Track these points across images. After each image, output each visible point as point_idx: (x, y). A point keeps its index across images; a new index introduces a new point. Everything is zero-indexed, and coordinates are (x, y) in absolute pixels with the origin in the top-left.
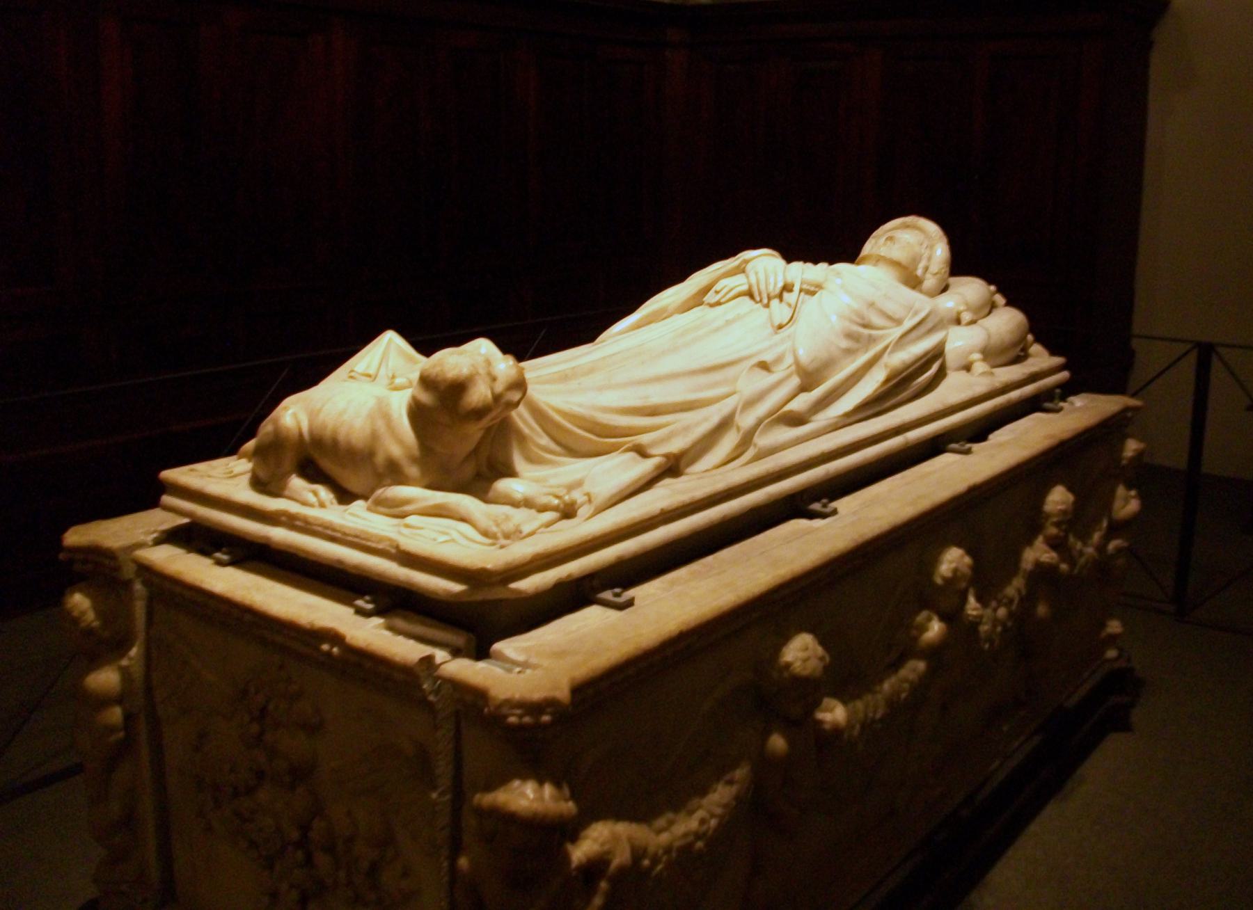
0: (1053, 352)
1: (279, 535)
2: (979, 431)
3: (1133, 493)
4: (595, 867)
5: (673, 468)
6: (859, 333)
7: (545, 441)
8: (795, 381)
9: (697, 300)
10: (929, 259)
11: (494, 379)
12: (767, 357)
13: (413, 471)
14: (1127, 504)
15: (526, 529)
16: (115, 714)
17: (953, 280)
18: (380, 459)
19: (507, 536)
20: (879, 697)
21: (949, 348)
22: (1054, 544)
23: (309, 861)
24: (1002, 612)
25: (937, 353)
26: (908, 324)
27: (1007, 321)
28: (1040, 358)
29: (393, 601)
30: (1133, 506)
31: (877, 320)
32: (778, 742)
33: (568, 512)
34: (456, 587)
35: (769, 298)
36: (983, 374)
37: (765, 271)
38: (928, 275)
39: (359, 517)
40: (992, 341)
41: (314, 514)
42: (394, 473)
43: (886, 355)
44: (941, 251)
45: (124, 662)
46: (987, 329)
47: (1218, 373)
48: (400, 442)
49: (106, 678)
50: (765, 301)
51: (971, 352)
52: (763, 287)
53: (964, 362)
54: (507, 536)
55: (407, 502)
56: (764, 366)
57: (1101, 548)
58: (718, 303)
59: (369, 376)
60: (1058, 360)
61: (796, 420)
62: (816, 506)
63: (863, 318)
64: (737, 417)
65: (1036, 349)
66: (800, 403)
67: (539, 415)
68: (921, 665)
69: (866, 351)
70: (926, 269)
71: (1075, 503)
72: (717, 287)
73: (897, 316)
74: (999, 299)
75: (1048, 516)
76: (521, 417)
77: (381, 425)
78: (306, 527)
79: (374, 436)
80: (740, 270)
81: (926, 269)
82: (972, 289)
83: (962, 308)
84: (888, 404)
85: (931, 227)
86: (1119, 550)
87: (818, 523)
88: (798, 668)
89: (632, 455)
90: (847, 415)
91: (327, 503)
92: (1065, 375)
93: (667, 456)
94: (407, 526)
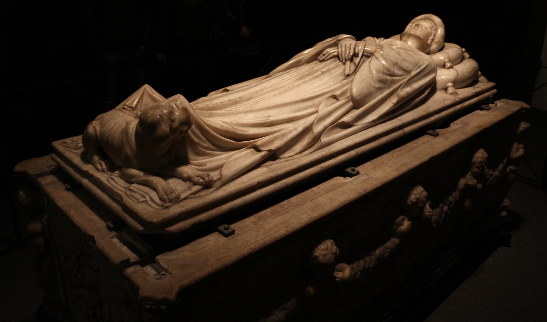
0: (489, 80)
1: (85, 181)
2: (445, 123)
3: (521, 146)
5: (273, 156)
6: (387, 79)
7: (207, 144)
8: (350, 104)
10: (435, 35)
11: (173, 121)
12: (337, 93)
14: (518, 151)
15: (183, 196)
16: (41, 240)
17: (446, 44)
19: (171, 201)
20: (373, 257)
21: (438, 79)
22: (475, 176)
24: (445, 208)
26: (413, 73)
27: (468, 66)
28: (483, 84)
30: (521, 152)
31: (397, 71)
32: (311, 290)
33: (207, 185)
34: (141, 228)
35: (346, 61)
36: (451, 94)
37: (346, 45)
38: (434, 43)
40: (459, 77)
43: (399, 90)
44: (440, 32)
45: (43, 220)
46: (457, 71)
48: (131, 148)
50: (344, 61)
51: (448, 82)
52: (343, 54)
53: (444, 86)
54: (171, 201)
55: (133, 176)
56: (335, 97)
58: (324, 60)
59: (132, 108)
60: (491, 84)
62: (349, 170)
63: (390, 72)
64: (314, 127)
65: (482, 78)
68: (397, 241)
69: (389, 88)
70: (433, 40)
71: (487, 158)
72: (324, 53)
73: (408, 70)
74: (467, 55)
75: (474, 163)
76: (193, 133)
80: (335, 45)
83: (446, 60)
85: (437, 20)
86: (512, 171)
87: (349, 179)
88: (321, 259)
89: (252, 150)
90: (374, 121)
91: (106, 170)
92: (495, 91)
93: (269, 151)
94: (130, 190)
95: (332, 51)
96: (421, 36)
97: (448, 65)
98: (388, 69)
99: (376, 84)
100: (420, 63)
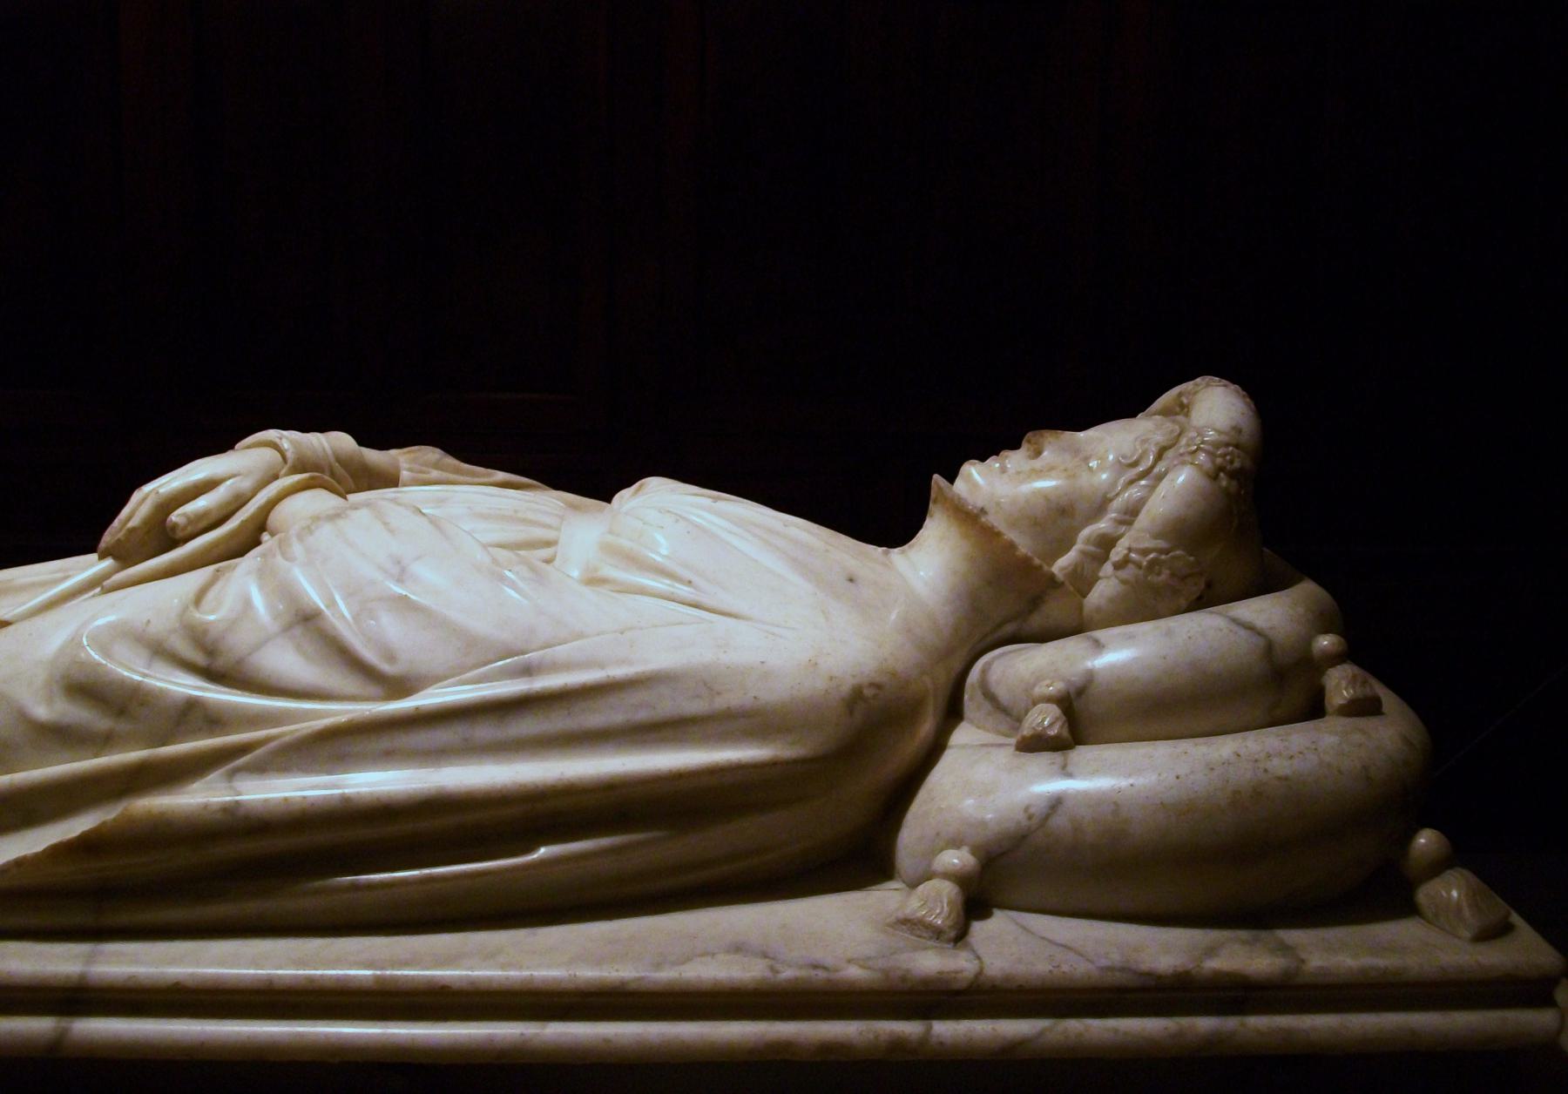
31: (287, 660)
38: (1108, 568)
40: (1060, 822)
43: (214, 776)
51: (955, 843)
63: (211, 651)
70: (1106, 543)
81: (1106, 543)
84: (124, 918)
96: (994, 520)
97: (1045, 718)
98: (199, 637)
99: (50, 701)
100: (561, 652)
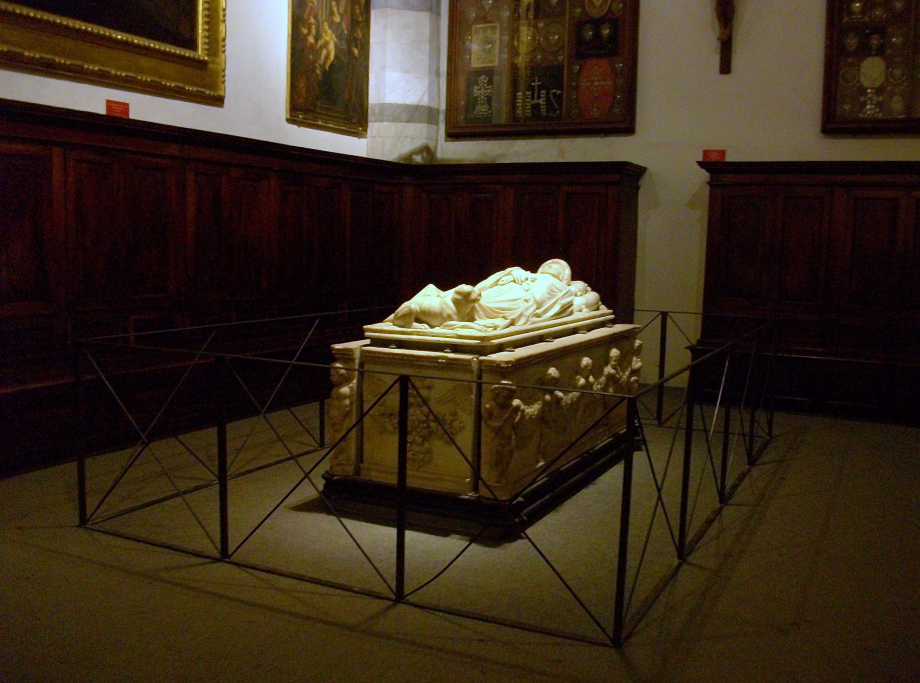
0: (609, 308)
4: (517, 408)
5: (512, 323)
8: (535, 306)
9: (496, 283)
12: (527, 298)
13: (455, 317)
16: (347, 402)
18: (445, 315)
21: (575, 303)
23: (428, 426)
25: (570, 304)
27: (593, 296)
28: (604, 309)
29: (455, 348)
39: (437, 330)
41: (421, 331)
42: (450, 318)
47: (669, 320)
49: (345, 390)
56: (526, 301)
57: (629, 377)
60: (611, 311)
61: (538, 316)
66: (538, 311)
67: (481, 306)
74: (589, 289)
77: (444, 306)
78: (424, 334)
79: (442, 309)
80: (509, 274)
82: (580, 285)
85: (564, 263)
92: (613, 316)
95: (510, 278)
97: (579, 293)
